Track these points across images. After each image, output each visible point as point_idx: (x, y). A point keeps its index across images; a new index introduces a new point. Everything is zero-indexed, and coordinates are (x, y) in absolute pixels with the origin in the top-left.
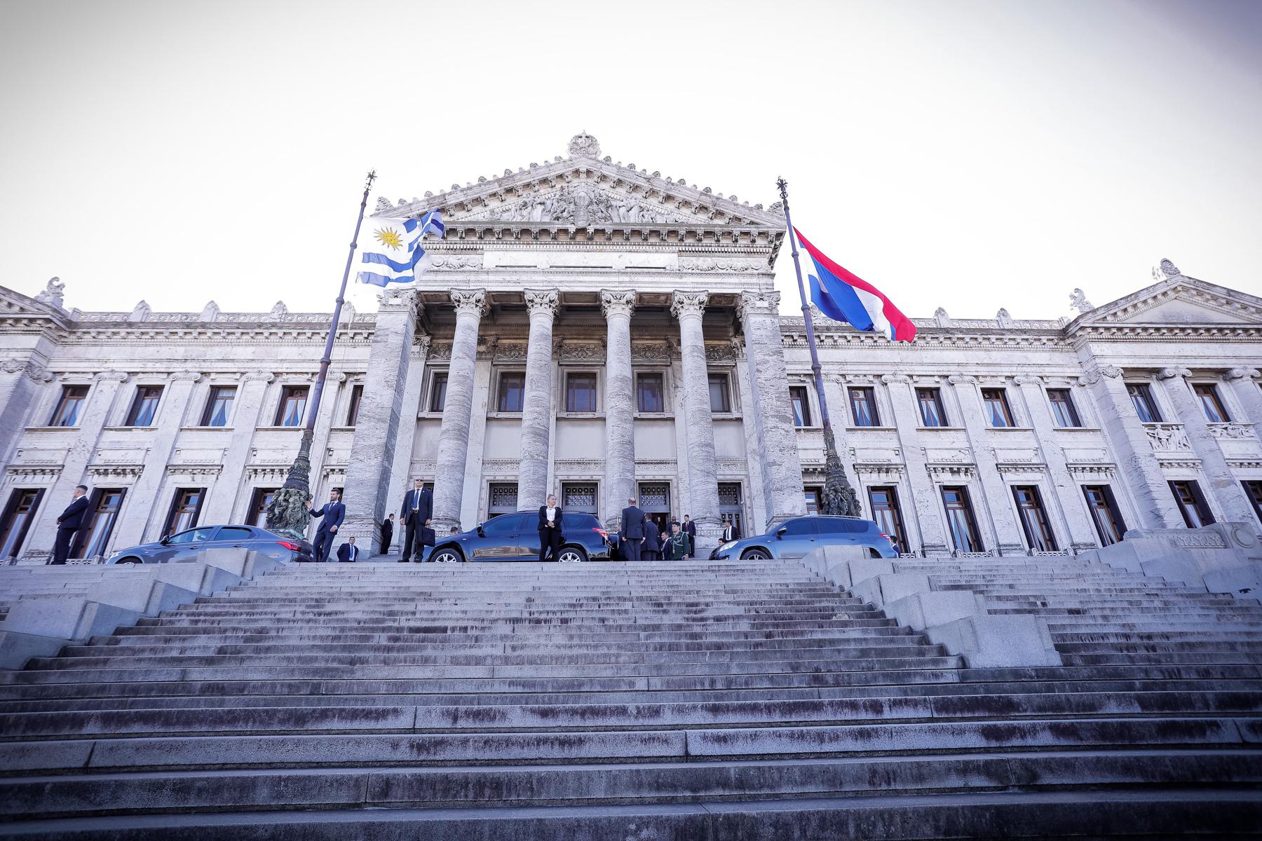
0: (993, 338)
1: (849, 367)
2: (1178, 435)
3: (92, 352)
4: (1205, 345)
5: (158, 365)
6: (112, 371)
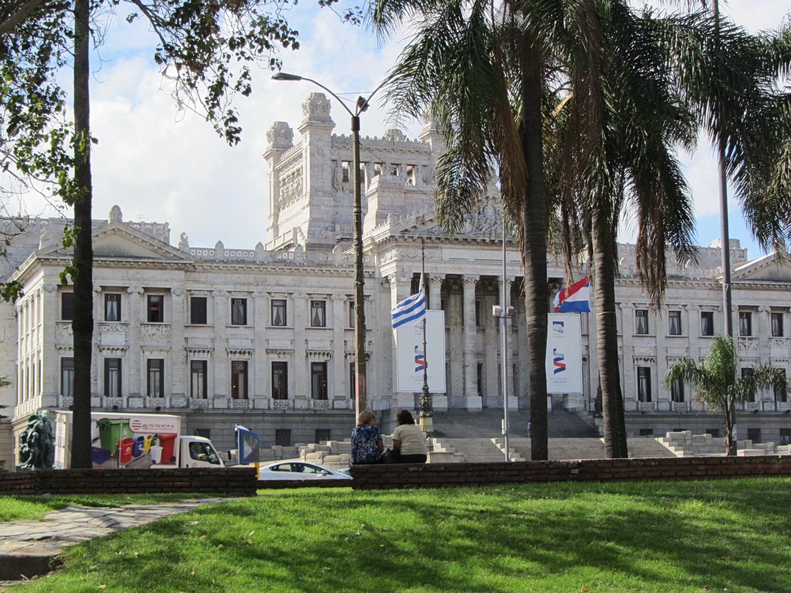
0: (681, 282)
3: (203, 277)
5: (243, 287)
6: (220, 291)
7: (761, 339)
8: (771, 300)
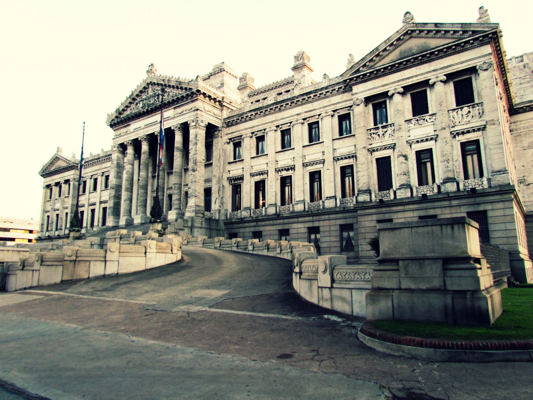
0: (312, 95)
1: (254, 128)
2: (390, 130)
4: (419, 67)
7: (395, 125)
8: (403, 80)
